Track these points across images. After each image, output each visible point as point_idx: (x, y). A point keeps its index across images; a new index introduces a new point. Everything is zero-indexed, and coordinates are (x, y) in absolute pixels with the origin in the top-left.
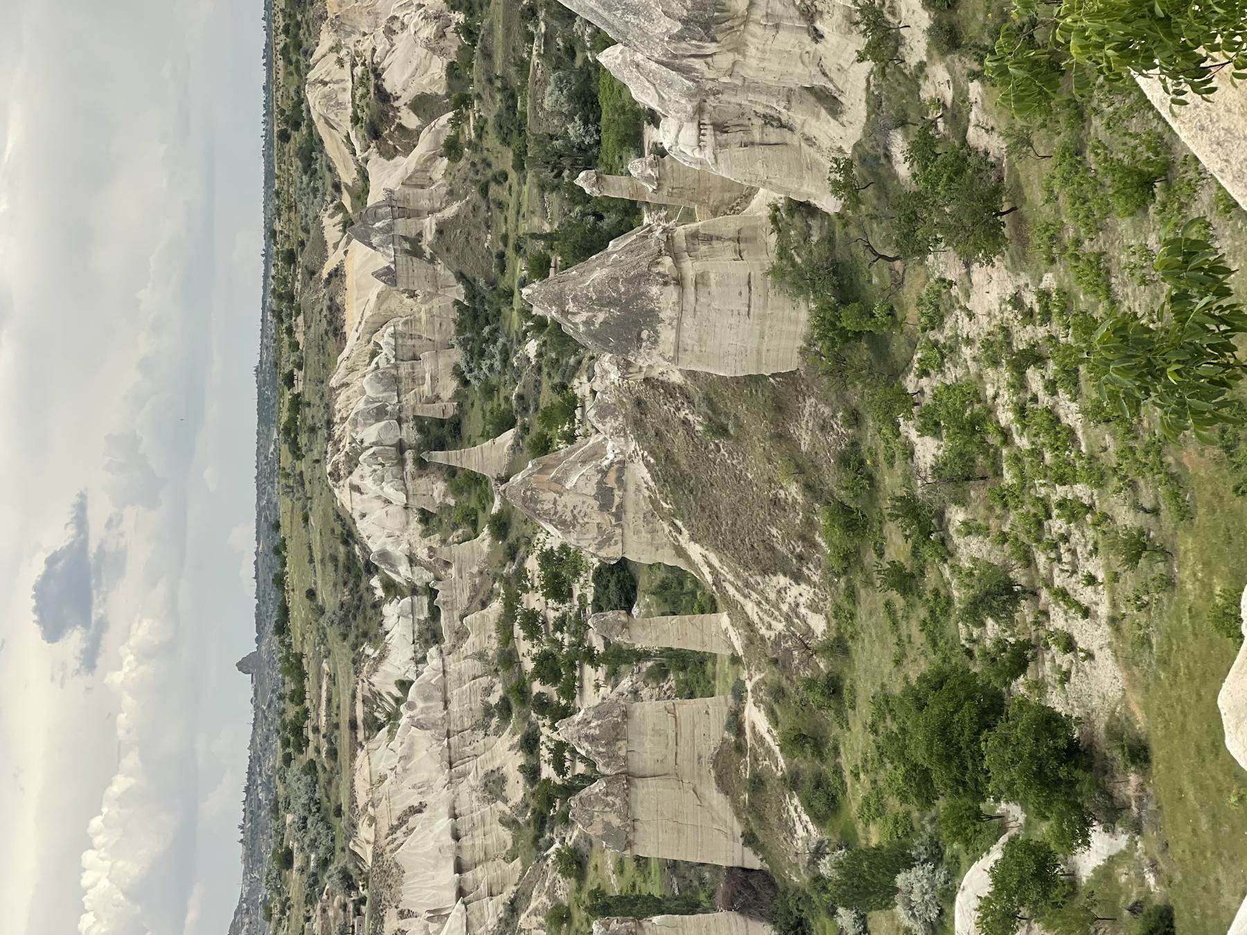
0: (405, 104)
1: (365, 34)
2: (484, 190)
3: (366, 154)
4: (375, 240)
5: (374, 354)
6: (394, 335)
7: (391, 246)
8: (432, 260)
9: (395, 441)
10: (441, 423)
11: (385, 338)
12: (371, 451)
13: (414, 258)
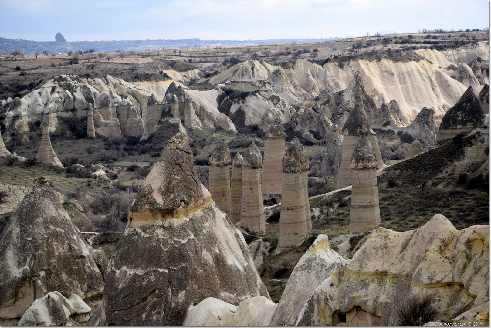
4: (169, 95)
5: (122, 96)
6: (128, 105)
7: (167, 102)
8: (160, 122)
9: (76, 107)
10: (85, 129)
11: (129, 100)
12: (71, 96)
13: (161, 113)
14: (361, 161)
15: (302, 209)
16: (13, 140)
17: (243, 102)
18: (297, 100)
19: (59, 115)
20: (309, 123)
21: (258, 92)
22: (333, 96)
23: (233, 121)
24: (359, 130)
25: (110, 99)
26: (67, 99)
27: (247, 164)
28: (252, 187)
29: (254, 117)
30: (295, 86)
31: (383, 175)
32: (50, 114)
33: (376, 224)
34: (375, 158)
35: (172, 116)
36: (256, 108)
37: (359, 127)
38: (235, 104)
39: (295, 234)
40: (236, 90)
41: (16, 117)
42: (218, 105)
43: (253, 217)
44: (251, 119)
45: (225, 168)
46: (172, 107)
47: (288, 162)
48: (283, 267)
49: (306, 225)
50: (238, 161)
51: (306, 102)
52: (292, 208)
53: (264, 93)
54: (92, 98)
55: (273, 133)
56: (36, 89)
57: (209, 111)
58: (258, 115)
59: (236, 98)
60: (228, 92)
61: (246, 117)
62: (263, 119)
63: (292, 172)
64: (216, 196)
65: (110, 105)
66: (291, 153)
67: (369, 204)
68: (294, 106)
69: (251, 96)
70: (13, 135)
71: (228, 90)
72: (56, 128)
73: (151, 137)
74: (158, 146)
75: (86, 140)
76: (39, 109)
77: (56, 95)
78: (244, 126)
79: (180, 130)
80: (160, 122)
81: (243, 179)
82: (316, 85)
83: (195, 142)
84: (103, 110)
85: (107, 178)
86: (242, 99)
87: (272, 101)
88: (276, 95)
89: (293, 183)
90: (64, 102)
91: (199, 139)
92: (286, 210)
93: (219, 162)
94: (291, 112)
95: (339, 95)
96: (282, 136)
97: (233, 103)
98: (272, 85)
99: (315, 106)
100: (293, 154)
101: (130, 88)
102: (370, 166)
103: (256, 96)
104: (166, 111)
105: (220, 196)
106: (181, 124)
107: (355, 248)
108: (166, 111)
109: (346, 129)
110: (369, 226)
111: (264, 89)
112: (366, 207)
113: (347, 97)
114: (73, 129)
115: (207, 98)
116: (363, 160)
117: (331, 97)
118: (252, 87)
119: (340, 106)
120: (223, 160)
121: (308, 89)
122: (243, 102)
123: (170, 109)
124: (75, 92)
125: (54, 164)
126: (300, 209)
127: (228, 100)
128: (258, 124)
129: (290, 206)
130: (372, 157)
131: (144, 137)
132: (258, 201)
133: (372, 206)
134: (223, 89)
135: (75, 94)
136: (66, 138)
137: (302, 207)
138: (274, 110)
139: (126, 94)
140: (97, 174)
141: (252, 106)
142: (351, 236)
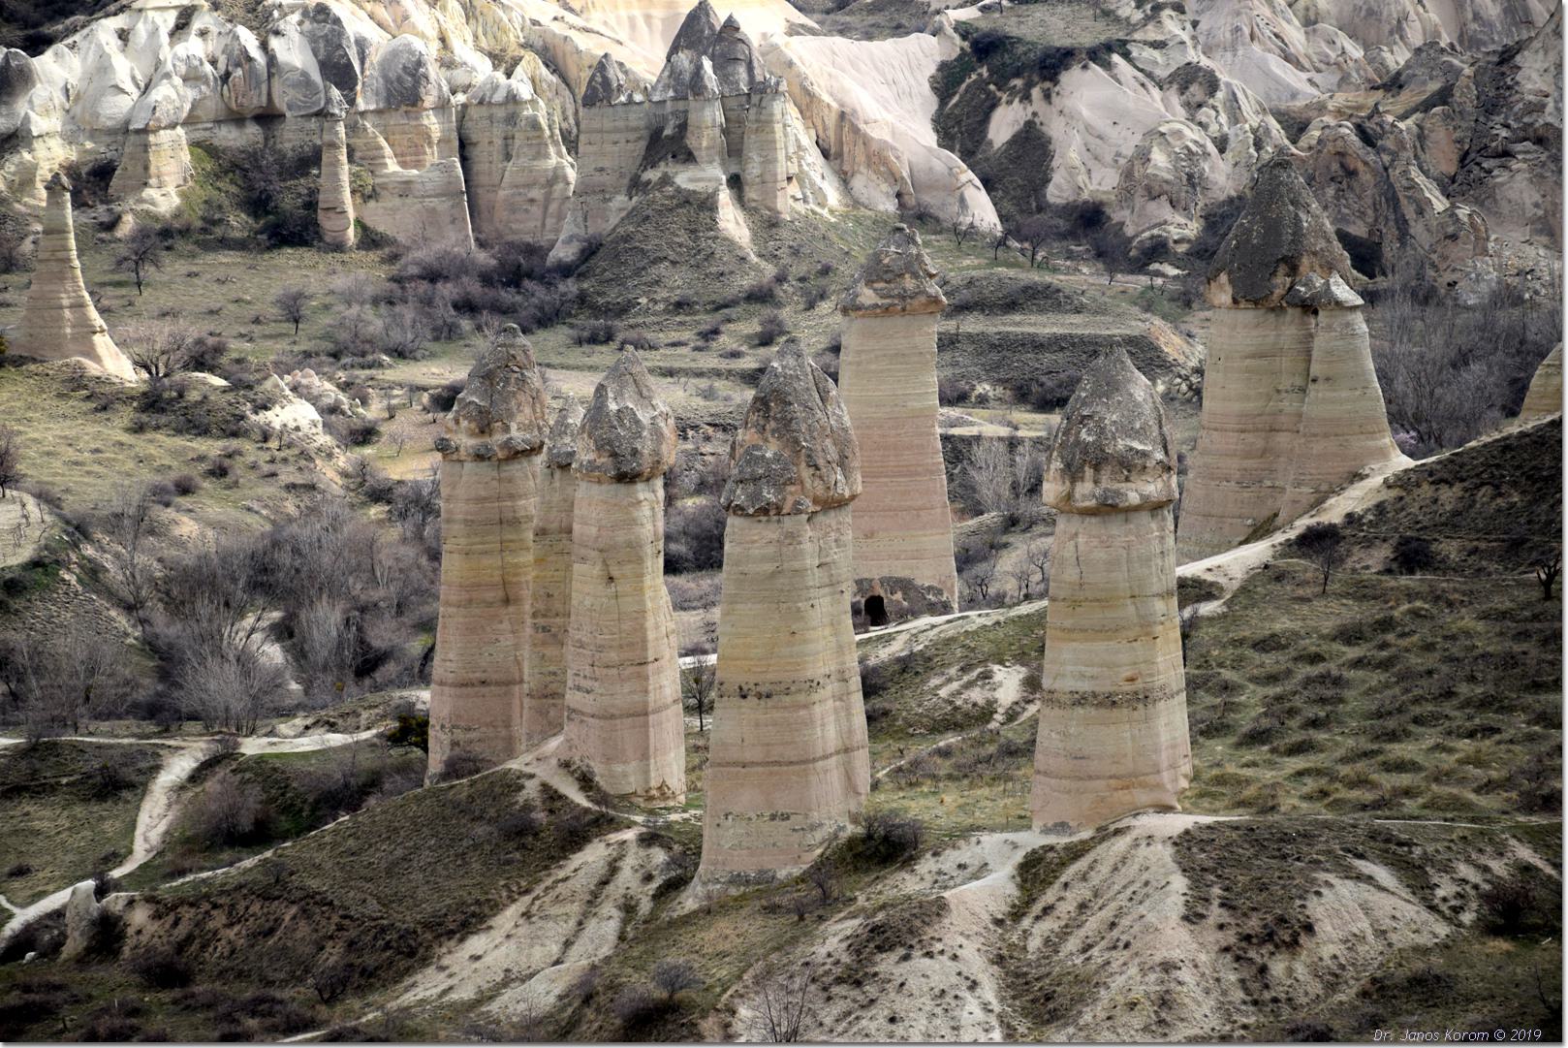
0: (1035, 114)
1: (1195, 24)
2: (760, 296)
3: (950, 31)
4: (684, 59)
5: (495, 58)
6: (512, 98)
7: (671, 93)
8: (636, 185)
9: (281, 103)
12: (255, 52)
13: (643, 144)
14: (1089, 472)
15: (815, 697)
17: (1047, 96)
18: (1301, 86)
19: (199, 135)
20: (1337, 198)
21: (1122, 48)
22: (1468, 71)
23: (988, 184)
24: (1281, 281)
25: (433, 70)
26: (238, 65)
27: (591, 456)
28: (615, 572)
29: (1091, 164)
30: (1309, 22)
31: (1380, 508)
32: (155, 131)
33: (1159, 786)
34: (1159, 456)
35: (689, 157)
36: (1102, 124)
37: (1282, 269)
38: (1009, 103)
39: (773, 817)
40: (1019, 40)
42: (935, 107)
43: (612, 717)
45: (515, 469)
46: (692, 118)
47: (748, 462)
48: (661, 994)
49: (835, 778)
50: (567, 440)
51: (1341, 99)
52: (763, 689)
53: (1149, 53)
54: (349, 65)
55: (882, 285)
56: (107, 16)
57: (875, 133)
58: (1108, 158)
59: (1017, 74)
60: (984, 47)
61: (1054, 164)
62: (1128, 175)
63: (764, 511)
64: (470, 601)
65: (429, 100)
66: (767, 418)
67: (1128, 687)
68: (1282, 117)
69: (1085, 67)
71: (987, 35)
72: (183, 195)
73: (591, 251)
74: (613, 295)
75: (308, 255)
76: (117, 107)
77: (193, 47)
79: (722, 225)
80: (636, 185)
81: (576, 527)
82: (1413, 16)
83: (780, 279)
84: (396, 119)
85: (324, 439)
86: (1044, 79)
87: (1183, 90)
88: (1205, 62)
89: (769, 567)
90: (226, 77)
91: (800, 268)
92: (737, 701)
93: (487, 439)
94: (1258, 145)
95: (1500, 63)
96: (923, 299)
97: (1005, 98)
98: (1190, 16)
99: (1370, 117)
100: (773, 424)
101: (535, 23)
102: (1134, 498)
104: (668, 132)
105: (490, 604)
106: (725, 196)
107: (1037, 908)
108: (668, 132)
109: (1223, 278)
110: (1123, 796)
111: (1151, 33)
112: (1110, 702)
113: (1535, 76)
114: (258, 204)
115: (883, 75)
116: (1097, 468)
117: (1458, 72)
118: (1101, 25)
119: (1500, 119)
120: (507, 429)
121: (1372, 35)
122: (1047, 96)
123: (683, 127)
124: (277, 33)
125: (93, 369)
126: (801, 698)
127: (981, 85)
128: (1104, 198)
129: (753, 680)
130: (1144, 454)
131: (564, 252)
132: (644, 641)
133: (1143, 698)
134: (964, 30)
135: (274, 43)
137: (813, 685)
138: (1178, 134)
139: (513, 50)
140: (277, 425)
141: (1085, 112)
142: (1032, 840)
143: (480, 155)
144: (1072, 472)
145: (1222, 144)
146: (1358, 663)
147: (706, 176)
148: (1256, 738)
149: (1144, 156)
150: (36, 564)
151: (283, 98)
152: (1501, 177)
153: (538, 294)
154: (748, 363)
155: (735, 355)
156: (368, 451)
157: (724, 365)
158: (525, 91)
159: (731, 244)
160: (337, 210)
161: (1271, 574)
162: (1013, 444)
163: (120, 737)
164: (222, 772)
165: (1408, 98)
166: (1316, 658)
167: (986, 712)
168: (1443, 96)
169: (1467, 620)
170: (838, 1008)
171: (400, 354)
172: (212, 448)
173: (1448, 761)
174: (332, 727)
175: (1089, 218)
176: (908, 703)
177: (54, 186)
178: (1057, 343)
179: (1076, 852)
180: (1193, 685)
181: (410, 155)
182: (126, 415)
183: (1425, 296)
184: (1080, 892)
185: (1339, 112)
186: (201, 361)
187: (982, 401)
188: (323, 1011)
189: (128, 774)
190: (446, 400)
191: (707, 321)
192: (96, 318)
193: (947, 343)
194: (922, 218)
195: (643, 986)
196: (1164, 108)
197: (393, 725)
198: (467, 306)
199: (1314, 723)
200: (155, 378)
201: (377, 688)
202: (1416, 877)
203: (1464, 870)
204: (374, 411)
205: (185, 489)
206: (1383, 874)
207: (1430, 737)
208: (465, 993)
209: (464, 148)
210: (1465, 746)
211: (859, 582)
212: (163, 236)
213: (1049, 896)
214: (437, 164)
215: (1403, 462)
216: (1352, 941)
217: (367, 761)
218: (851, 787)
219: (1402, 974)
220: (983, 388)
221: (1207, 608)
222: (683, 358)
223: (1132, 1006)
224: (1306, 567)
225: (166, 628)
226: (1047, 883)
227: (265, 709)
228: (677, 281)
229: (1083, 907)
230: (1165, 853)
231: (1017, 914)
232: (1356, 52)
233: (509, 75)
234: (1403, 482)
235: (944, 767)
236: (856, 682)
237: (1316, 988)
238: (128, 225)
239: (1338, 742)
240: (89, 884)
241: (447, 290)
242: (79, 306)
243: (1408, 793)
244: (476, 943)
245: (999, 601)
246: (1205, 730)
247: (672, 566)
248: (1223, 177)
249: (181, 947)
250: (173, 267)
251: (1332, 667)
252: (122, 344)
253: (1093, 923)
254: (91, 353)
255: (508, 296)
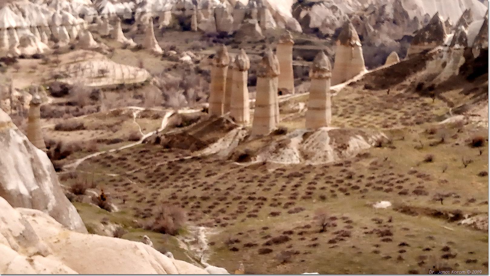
6: (223, 8)
10: (190, 24)
16: (139, 29)
18: (351, 10)
21: (323, 2)
23: (301, 24)
32: (166, 11)
41: (143, 13)
44: (315, 23)
57: (282, 15)
65: (209, 7)
68: (348, 15)
70: (139, 26)
76: (159, 8)
78: (309, 28)
84: (204, 10)
103: (320, 5)
114: (182, 24)
122: (310, 10)
127: (299, 8)
136: (176, 30)
143: (218, 17)
144: (314, 72)
145: (338, 18)
146: (358, 104)
147: (254, 21)
148: (341, 115)
149: (325, 20)
150: (146, 81)
151: (186, 7)
152: (382, 26)
153: (226, 40)
154: (260, 52)
155: (258, 51)
156: (198, 65)
157: (257, 52)
158: (225, 6)
159: (257, 32)
160: (194, 25)
161: (345, 89)
162: (303, 67)
163: (157, 109)
164: (175, 116)
165: (368, 12)
166: (351, 103)
167: (298, 110)
168: (374, 12)
169: (375, 97)
170: (273, 156)
171: (204, 49)
172: (174, 63)
173: (371, 120)
174: (192, 109)
175: (316, 31)
176: (285, 108)
177: (150, 20)
178: (311, 50)
179: (312, 133)
180: (332, 107)
181: (206, 16)
182: (160, 58)
183: (370, 45)
184: (313, 139)
185: (357, 14)
186: (172, 49)
187: (298, 60)
188: (191, 153)
189: (161, 115)
190: (211, 57)
191: (254, 45)
192: (156, 41)
193: (294, 50)
194: (289, 29)
195: (242, 151)
196: (329, 12)
197: (202, 109)
198: (214, 41)
199: (351, 113)
200: (165, 52)
201: (200, 103)
202: (366, 138)
203: (373, 137)
204: (199, 58)
205: (169, 70)
206: (361, 137)
207: (369, 116)
208: (214, 152)
209: (215, 15)
210: (374, 118)
211: (278, 89)
212: (167, 29)
213: (307, 140)
214: (211, 18)
215: (365, 71)
216: (355, 148)
217: (198, 115)
218: (276, 122)
219: (363, 153)
220: (298, 57)
221: (335, 94)
222: (250, 51)
223: (320, 157)
224: (350, 88)
225: (166, 92)
226: (307, 138)
227: (181, 106)
228: (249, 38)
229: (313, 142)
230: (327, 134)
231: (302, 142)
232: (360, 4)
233: (223, 3)
234: (366, 75)
235: (291, 119)
236: (278, 105)
237: (349, 155)
238: (161, 27)
239: (354, 117)
240: (155, 132)
241: (211, 39)
242: (153, 40)
243: (365, 125)
244: (215, 144)
245: (301, 92)
246: (333, 114)
247: (248, 85)
248: (338, 24)
249: (170, 142)
250: (168, 34)
251: (354, 104)
252: (160, 46)
253: (314, 144)
254: (155, 47)
255: (221, 40)
